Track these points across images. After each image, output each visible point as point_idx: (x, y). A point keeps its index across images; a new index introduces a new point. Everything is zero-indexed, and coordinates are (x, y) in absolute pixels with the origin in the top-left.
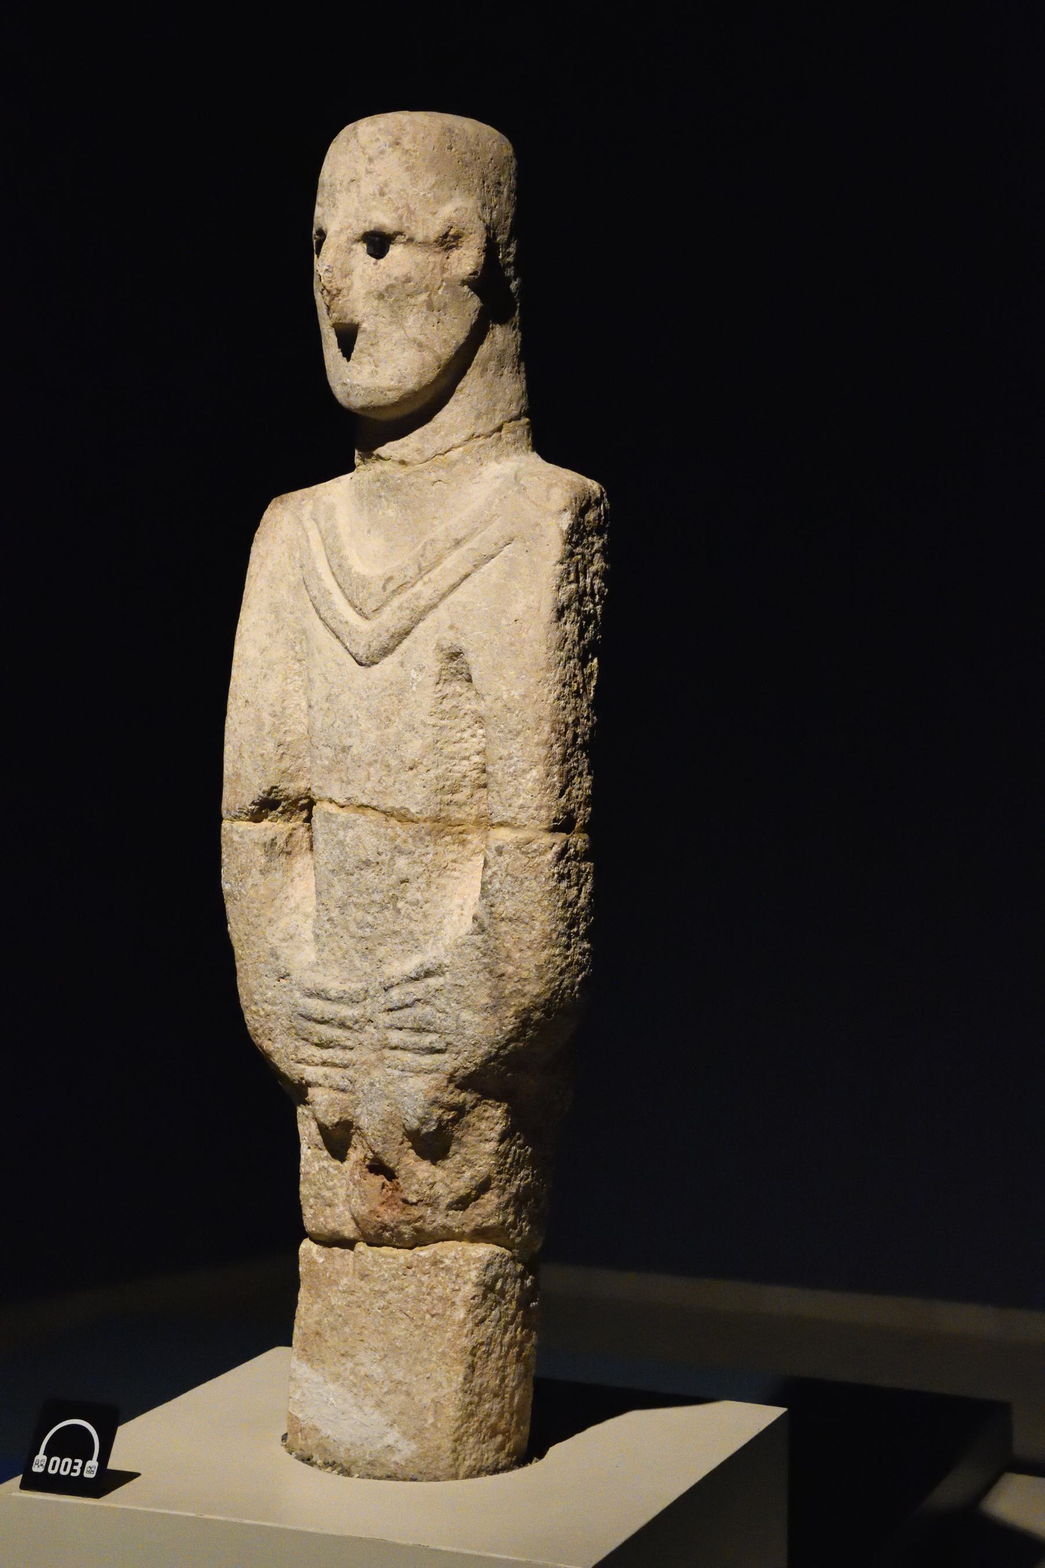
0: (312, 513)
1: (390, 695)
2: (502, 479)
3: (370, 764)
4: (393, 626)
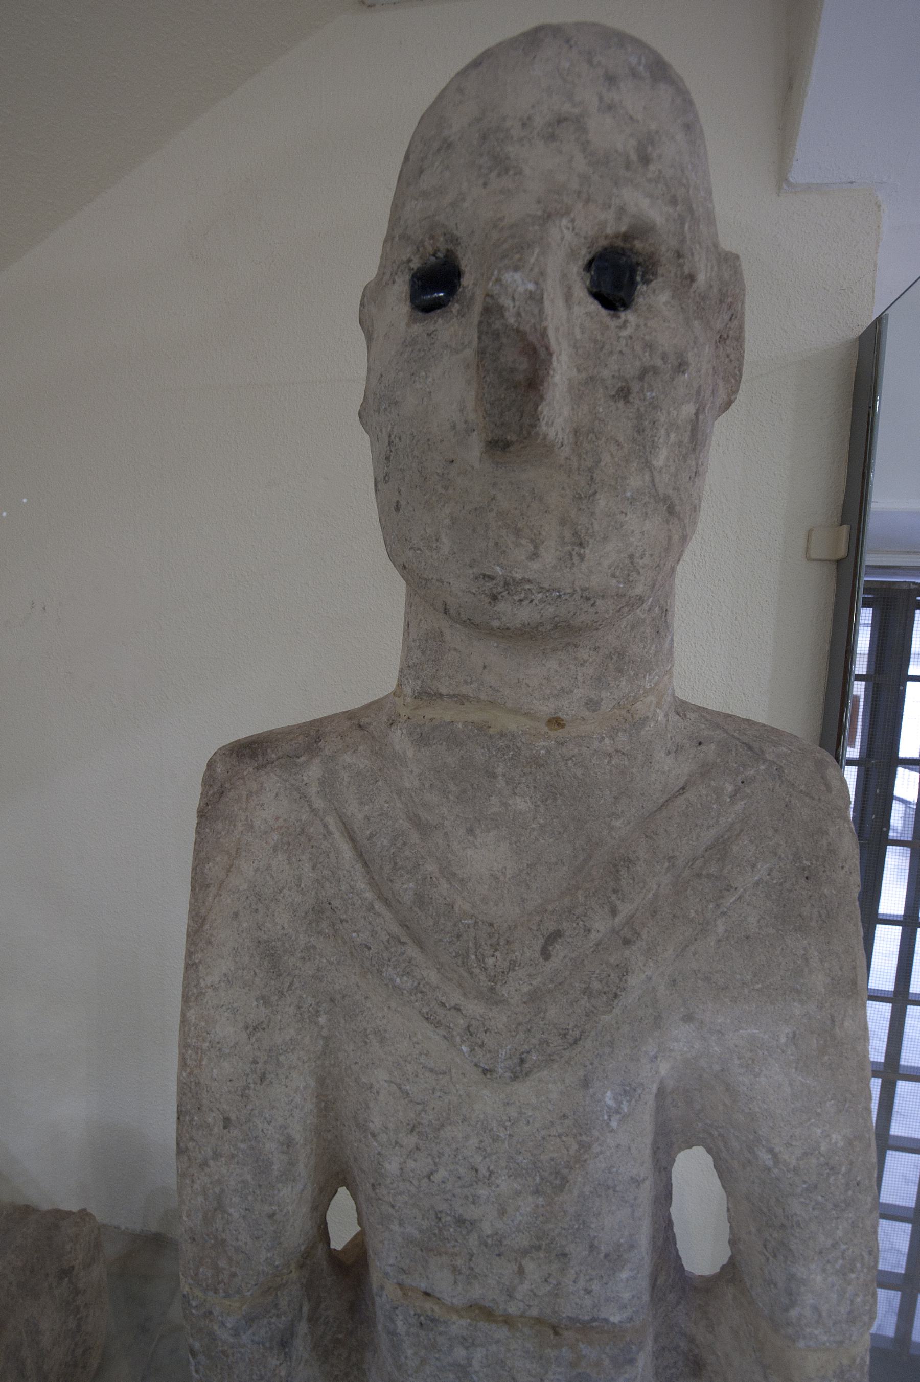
0: (322, 782)
1: (560, 1136)
2: (713, 746)
3: (525, 1252)
4: (576, 1026)
